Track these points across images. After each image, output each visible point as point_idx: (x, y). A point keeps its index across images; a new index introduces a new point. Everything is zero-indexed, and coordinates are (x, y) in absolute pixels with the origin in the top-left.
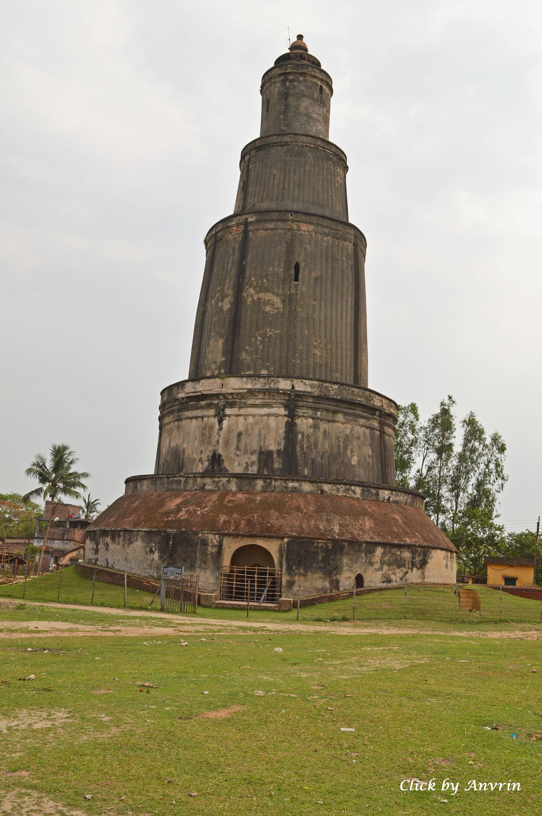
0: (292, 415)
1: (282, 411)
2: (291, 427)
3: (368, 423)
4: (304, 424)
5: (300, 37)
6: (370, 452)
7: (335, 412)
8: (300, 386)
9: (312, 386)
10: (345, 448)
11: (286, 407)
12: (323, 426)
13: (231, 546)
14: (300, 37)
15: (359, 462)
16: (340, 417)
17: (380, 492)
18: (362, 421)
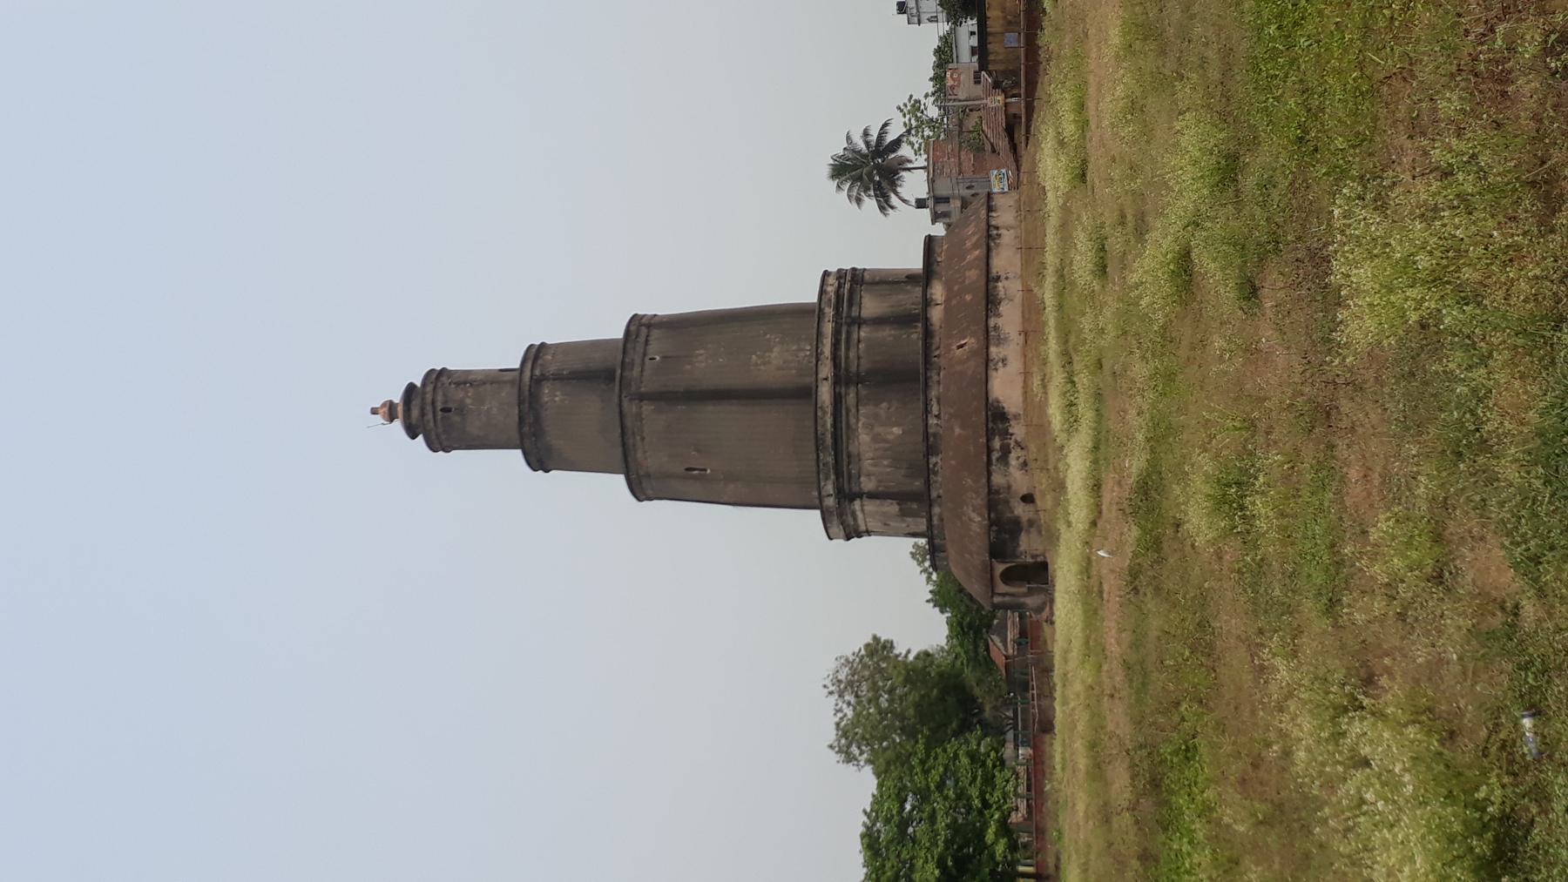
0: (860, 495)
1: (857, 504)
2: (873, 496)
3: (853, 410)
4: (868, 484)
5: (390, 412)
6: (884, 405)
7: (849, 456)
8: (829, 488)
9: (827, 479)
10: (886, 441)
11: (852, 500)
12: (867, 464)
13: (1002, 588)
14: (390, 412)
15: (898, 425)
16: (853, 449)
17: (931, 431)
18: (853, 421)
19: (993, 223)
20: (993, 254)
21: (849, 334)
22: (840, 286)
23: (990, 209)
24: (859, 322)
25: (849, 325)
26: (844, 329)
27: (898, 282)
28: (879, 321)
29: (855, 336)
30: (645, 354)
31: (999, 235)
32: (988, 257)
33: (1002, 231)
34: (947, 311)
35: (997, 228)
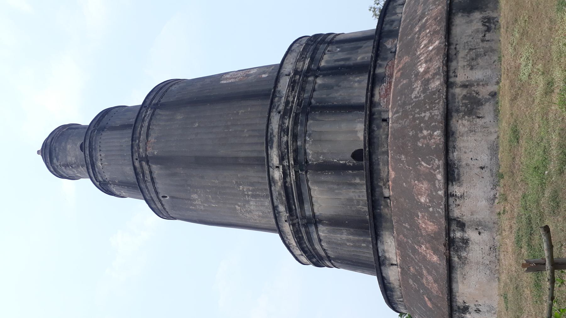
19: (456, 213)
20: (458, 275)
21: (308, 234)
22: (285, 175)
23: (451, 174)
24: (315, 221)
25: (306, 226)
26: (303, 230)
27: (344, 168)
28: (335, 222)
29: (315, 236)
30: (157, 193)
31: (466, 242)
32: (450, 280)
33: (471, 234)
34: (404, 272)
35: (462, 226)
